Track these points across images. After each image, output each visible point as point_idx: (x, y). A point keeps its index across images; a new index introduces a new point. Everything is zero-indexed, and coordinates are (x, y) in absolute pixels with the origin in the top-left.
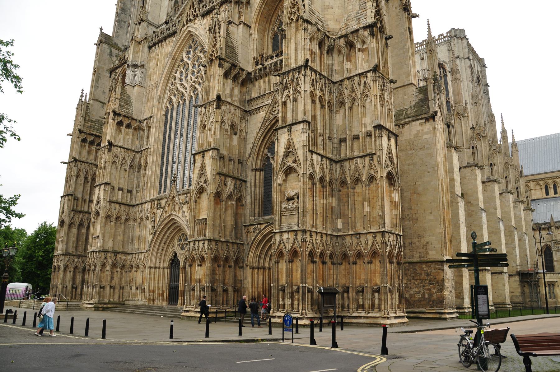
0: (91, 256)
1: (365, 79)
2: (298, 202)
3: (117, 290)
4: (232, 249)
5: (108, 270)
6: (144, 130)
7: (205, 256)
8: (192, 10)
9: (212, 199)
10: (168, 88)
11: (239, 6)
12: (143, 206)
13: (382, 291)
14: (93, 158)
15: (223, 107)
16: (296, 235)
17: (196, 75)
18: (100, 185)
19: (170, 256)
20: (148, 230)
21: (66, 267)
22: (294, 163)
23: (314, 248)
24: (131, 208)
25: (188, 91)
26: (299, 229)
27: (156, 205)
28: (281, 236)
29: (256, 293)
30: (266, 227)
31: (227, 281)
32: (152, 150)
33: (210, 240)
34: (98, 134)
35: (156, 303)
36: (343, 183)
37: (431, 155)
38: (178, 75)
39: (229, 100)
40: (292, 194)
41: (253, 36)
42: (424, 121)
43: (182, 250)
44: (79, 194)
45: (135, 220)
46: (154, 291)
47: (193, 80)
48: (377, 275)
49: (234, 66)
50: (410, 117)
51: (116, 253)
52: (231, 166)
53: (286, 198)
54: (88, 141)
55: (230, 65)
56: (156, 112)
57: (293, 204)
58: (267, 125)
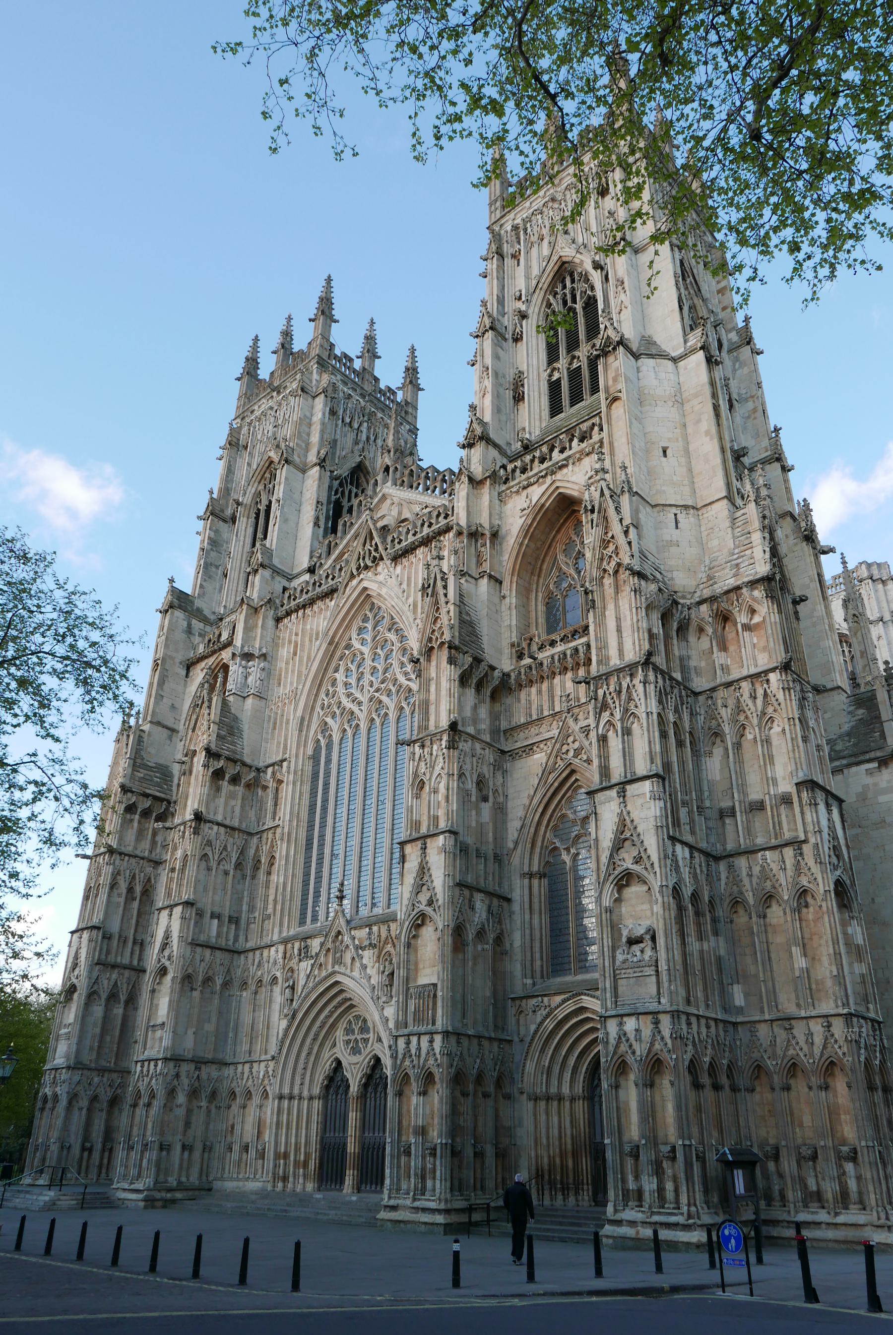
0: (142, 1071)
1: (765, 686)
2: (654, 948)
3: (197, 1154)
4: (491, 1050)
5: (180, 1106)
6: (265, 788)
7: (436, 1071)
8: (368, 546)
9: (449, 940)
11: (476, 541)
12: (266, 952)
14: (148, 846)
15: (461, 745)
16: (657, 1023)
18: (171, 907)
19: (325, 1067)
20: (276, 1007)
21: (73, 1098)
22: (637, 863)
23: (697, 1051)
24: (236, 956)
26: (661, 1008)
27: (296, 951)
28: (621, 1024)
29: (546, 1160)
30: (564, 1001)
31: (480, 1129)
32: (286, 830)
34: (158, 794)
35: (290, 1185)
39: (471, 730)
41: (507, 600)
42: (876, 765)
43: (355, 1054)
44: (115, 927)
45: (244, 985)
46: (286, 1156)
47: (376, 686)
48: (843, 1117)
49: (477, 660)
50: (844, 758)
51: (199, 1062)
52: (482, 867)
53: (624, 940)
54: (139, 810)
55: (470, 659)
56: (294, 752)
57: (642, 951)
58: (550, 780)
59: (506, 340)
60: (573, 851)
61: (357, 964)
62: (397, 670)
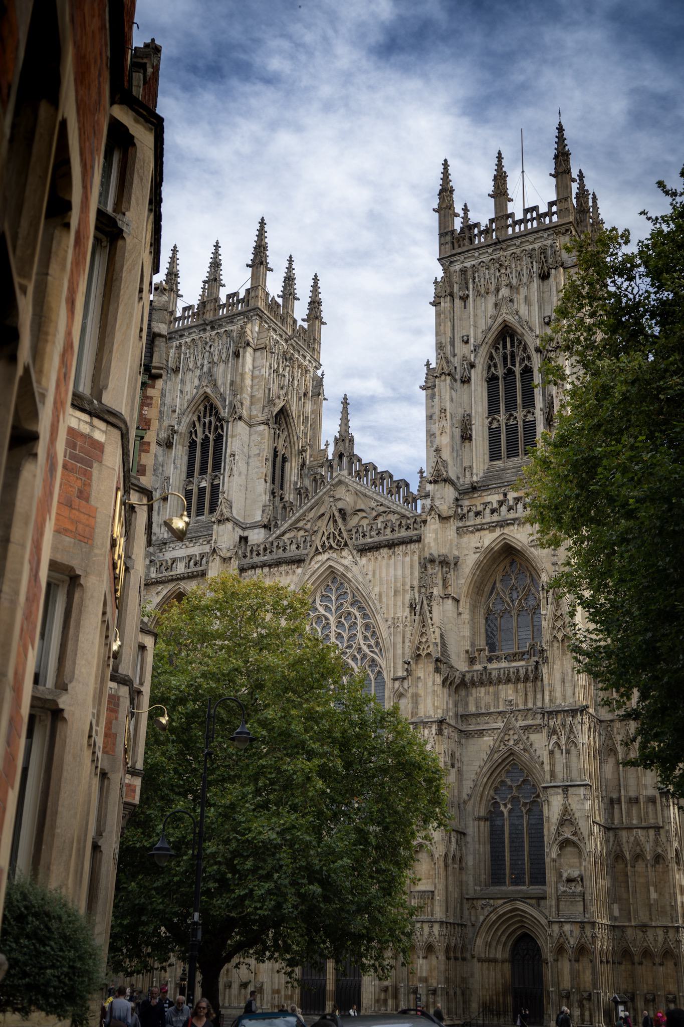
9: (442, 864)
17: (345, 645)
28: (561, 927)
29: (488, 998)
30: (504, 903)
33: (442, 923)
40: (576, 874)
41: (463, 616)
53: (564, 878)
58: (496, 756)
59: (455, 380)
60: (509, 806)
62: (362, 642)
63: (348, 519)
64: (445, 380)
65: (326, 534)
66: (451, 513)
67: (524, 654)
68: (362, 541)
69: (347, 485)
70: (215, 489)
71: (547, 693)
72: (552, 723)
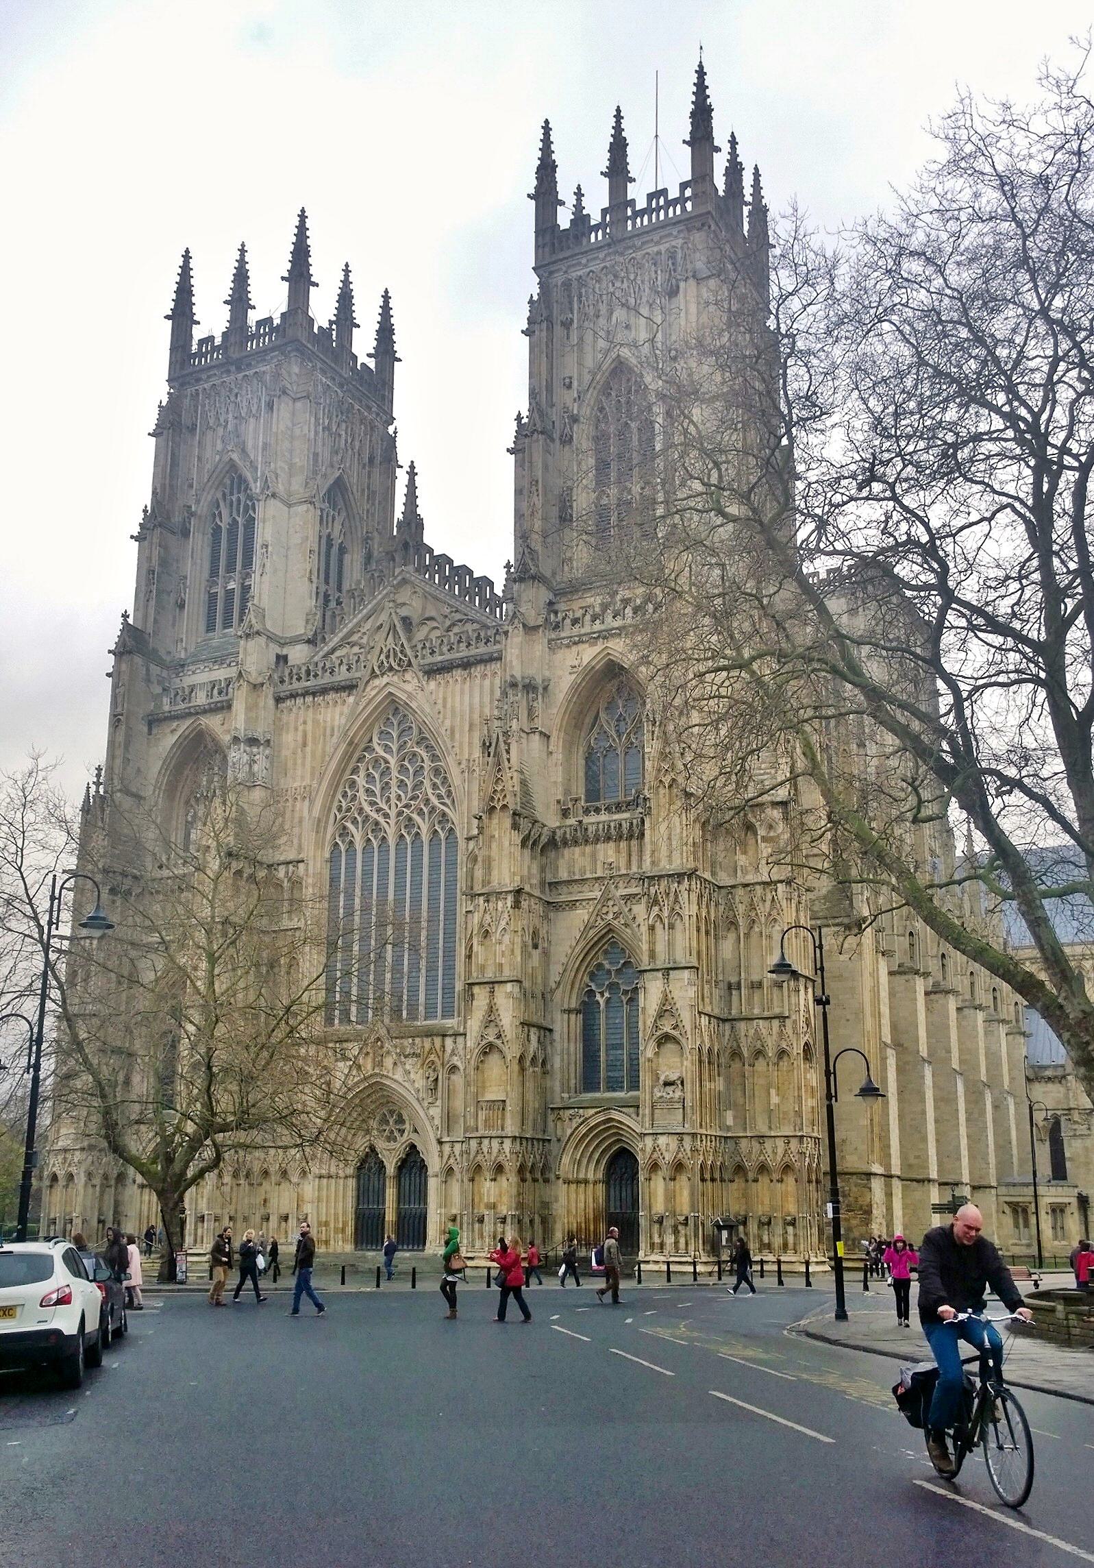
6: (279, 886)
9: (516, 1067)
10: (336, 804)
13: (799, 1223)
25: (392, 821)
33: (515, 1138)
36: (736, 1054)
37: (852, 990)
38: (361, 780)
40: (673, 1077)
41: (555, 755)
46: (326, 1224)
47: (404, 802)
53: (661, 1082)
56: (311, 854)
58: (592, 933)
59: (553, 440)
60: (607, 995)
61: (400, 1069)
62: (430, 791)
63: (415, 630)
64: (537, 441)
65: (385, 650)
66: (540, 621)
67: (628, 804)
68: (430, 659)
69: (414, 586)
70: (246, 589)
71: (647, 853)
72: (652, 890)
